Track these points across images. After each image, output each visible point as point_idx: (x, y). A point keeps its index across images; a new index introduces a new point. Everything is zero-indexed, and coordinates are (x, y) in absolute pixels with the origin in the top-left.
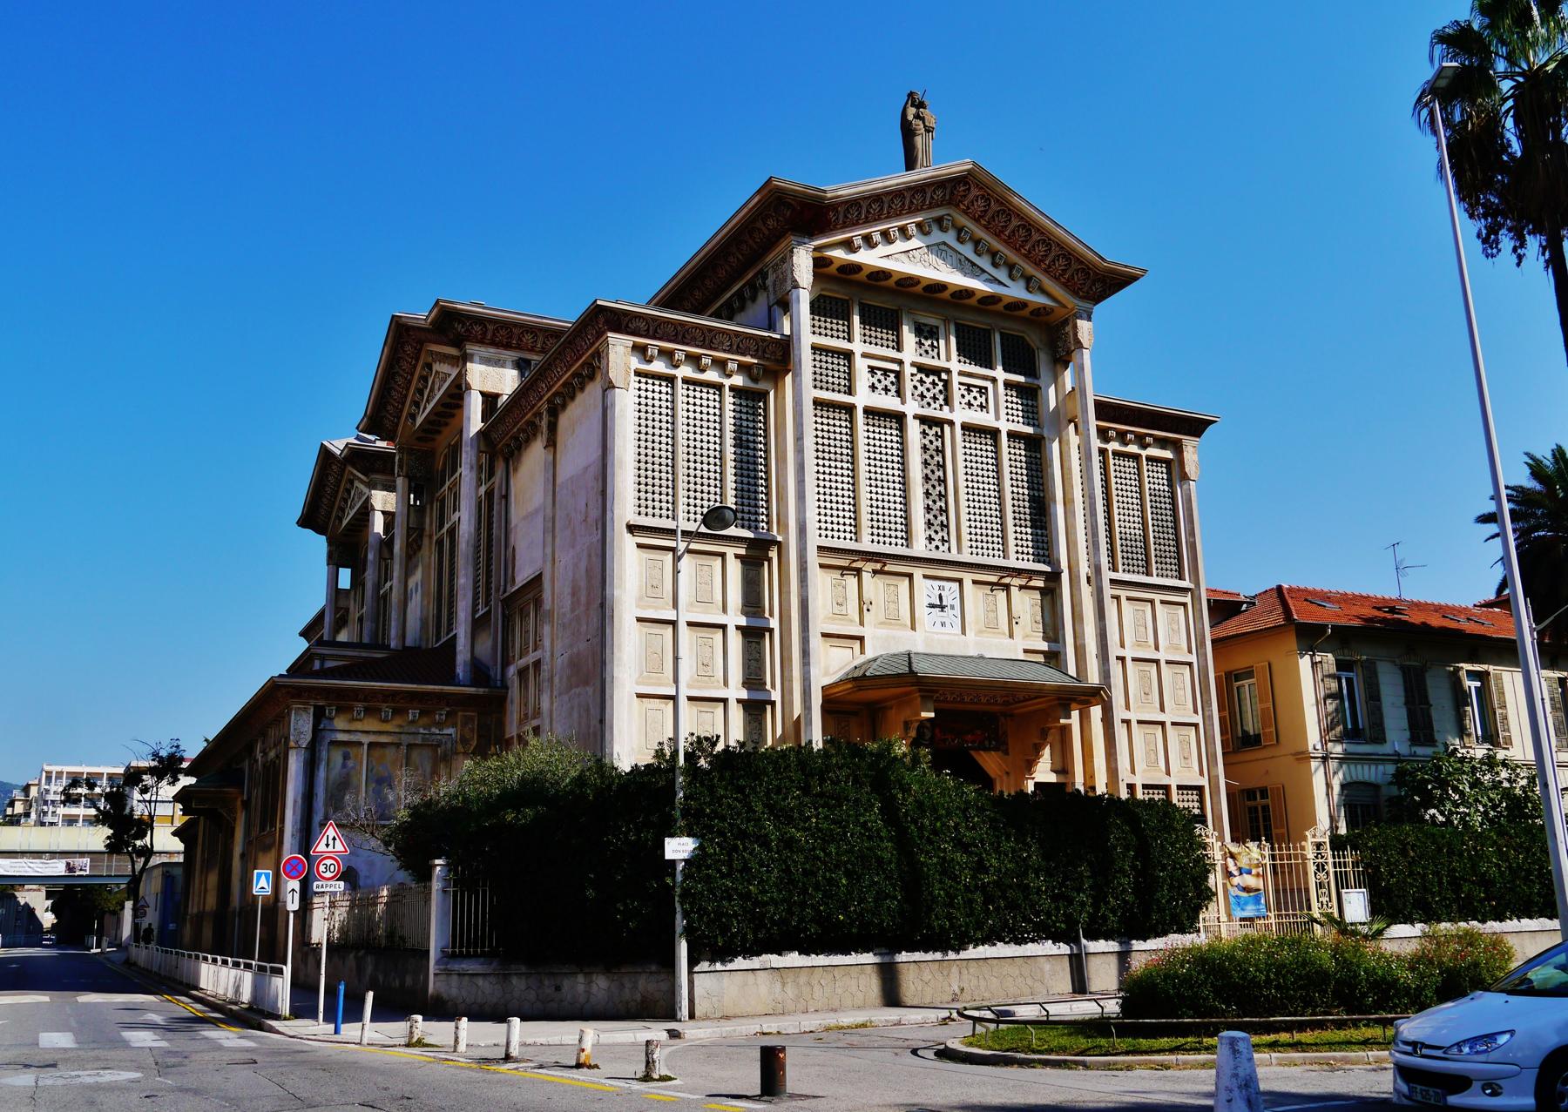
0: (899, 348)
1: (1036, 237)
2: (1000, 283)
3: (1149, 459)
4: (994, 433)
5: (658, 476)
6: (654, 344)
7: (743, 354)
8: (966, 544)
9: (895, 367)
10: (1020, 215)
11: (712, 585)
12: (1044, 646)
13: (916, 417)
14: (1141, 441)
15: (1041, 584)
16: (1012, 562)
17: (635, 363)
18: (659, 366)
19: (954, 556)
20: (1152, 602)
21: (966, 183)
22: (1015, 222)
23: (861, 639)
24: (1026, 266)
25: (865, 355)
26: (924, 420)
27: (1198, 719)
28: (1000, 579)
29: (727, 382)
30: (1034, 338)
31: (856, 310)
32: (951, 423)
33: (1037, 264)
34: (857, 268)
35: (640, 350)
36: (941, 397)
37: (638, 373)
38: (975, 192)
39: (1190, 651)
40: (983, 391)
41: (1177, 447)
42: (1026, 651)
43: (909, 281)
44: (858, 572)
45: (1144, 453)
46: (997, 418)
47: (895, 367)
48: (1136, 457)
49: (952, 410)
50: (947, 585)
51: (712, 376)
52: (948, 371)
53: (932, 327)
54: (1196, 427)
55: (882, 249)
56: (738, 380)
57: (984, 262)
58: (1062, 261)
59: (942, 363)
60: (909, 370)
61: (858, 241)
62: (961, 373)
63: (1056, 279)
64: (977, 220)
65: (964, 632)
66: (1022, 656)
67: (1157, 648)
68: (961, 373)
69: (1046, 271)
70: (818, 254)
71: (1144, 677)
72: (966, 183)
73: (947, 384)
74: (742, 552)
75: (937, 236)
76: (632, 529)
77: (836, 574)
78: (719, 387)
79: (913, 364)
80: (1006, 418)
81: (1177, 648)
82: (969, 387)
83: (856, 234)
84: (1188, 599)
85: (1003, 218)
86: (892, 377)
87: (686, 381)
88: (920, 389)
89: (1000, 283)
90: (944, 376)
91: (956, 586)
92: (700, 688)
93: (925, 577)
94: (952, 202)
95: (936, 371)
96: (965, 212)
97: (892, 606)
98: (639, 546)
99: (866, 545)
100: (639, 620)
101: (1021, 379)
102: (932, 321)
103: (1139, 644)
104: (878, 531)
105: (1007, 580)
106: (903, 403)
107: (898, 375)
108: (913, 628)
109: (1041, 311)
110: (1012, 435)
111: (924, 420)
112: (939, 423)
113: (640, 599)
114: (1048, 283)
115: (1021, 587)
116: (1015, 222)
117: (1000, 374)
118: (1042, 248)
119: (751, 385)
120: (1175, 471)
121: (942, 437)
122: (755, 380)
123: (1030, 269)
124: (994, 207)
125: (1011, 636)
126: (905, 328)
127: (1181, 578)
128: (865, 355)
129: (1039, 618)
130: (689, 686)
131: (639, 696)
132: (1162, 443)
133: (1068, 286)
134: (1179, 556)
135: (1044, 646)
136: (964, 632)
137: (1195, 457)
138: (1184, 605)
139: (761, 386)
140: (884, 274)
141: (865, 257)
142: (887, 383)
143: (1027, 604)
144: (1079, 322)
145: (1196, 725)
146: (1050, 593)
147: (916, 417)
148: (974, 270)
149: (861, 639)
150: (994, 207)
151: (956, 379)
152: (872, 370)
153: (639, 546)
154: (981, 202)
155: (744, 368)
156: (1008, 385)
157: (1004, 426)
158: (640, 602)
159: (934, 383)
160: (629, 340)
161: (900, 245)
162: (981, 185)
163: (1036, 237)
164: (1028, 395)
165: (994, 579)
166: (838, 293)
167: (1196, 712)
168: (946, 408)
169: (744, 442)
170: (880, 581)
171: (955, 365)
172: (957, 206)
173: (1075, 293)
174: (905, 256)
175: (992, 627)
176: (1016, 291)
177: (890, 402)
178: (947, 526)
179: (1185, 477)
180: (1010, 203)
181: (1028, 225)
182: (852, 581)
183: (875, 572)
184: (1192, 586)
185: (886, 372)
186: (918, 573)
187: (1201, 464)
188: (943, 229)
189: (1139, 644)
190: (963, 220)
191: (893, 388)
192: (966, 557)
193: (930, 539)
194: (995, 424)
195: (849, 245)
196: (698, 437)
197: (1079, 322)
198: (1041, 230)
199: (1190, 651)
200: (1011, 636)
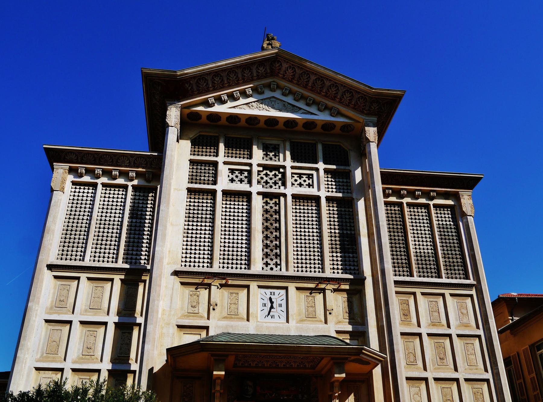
0: (250, 157)
1: (328, 83)
2: (312, 114)
3: (435, 206)
4: (317, 199)
5: (75, 237)
6: (82, 167)
7: (138, 167)
8: (291, 264)
9: (248, 168)
10: (315, 73)
11: (100, 300)
12: (349, 328)
13: (259, 193)
14: (427, 195)
15: (347, 287)
16: (328, 274)
17: (71, 178)
18: (87, 179)
19: (284, 272)
20: (443, 295)
21: (279, 62)
22: (313, 78)
23: (207, 328)
24: (327, 102)
25: (225, 163)
26: (265, 195)
27: (489, 376)
28: (317, 286)
29: (130, 184)
30: (346, 145)
31: (222, 140)
32: (285, 195)
33: (333, 99)
34: (216, 116)
35: (71, 171)
36: (280, 182)
37: (74, 183)
38: (285, 66)
39: (478, 327)
40: (310, 176)
41: (457, 197)
42: (338, 332)
43: (252, 119)
44: (209, 286)
45: (431, 203)
46: (319, 189)
47: (248, 168)
48: (427, 206)
49: (285, 187)
50: (277, 291)
51: (121, 181)
52: (284, 167)
53: (275, 145)
54: (470, 183)
55: (230, 104)
56: (135, 182)
57: (301, 104)
58: (348, 95)
59: (281, 163)
60: (255, 169)
61: (212, 101)
62: (292, 168)
63: (347, 106)
64: (291, 81)
65: (288, 321)
66: (334, 335)
67: (449, 326)
68: (292, 168)
69: (341, 102)
70: (187, 111)
71: (439, 347)
72: (279, 62)
73: (284, 174)
74: (123, 277)
75: (268, 94)
76: (51, 267)
77: (193, 288)
78: (125, 187)
79: (259, 165)
80: (324, 188)
81: (467, 326)
82: (300, 176)
83: (210, 97)
84: (473, 292)
85: (333, 89)
86: (246, 174)
87: (104, 185)
88: (265, 178)
89: (312, 114)
90: (281, 170)
91: (283, 292)
92: (80, 363)
93: (260, 287)
94: (273, 74)
95: (276, 168)
96: (283, 78)
97: (233, 306)
98: (56, 277)
99: (216, 268)
100: (47, 321)
101: (334, 167)
102: (275, 142)
103: (433, 324)
104: (226, 259)
105: (322, 286)
106: (251, 186)
107: (250, 172)
108: (248, 320)
109: (345, 127)
110: (328, 199)
111: (265, 195)
112: (277, 196)
113: (51, 308)
114: (343, 109)
115: (335, 290)
116: (313, 78)
117: (321, 166)
118: (333, 89)
119: (146, 184)
120: (457, 213)
121: (279, 204)
122: (148, 181)
123: (330, 104)
124: (298, 71)
125: (326, 322)
126: (255, 148)
127: (467, 278)
128: (225, 163)
129: (347, 311)
130: (74, 362)
131: (37, 369)
132: (446, 196)
133: (355, 108)
134: (463, 264)
135: (349, 328)
136: (288, 321)
137: (471, 202)
138: (471, 296)
139: (152, 184)
140: (233, 118)
141: (218, 108)
142: (242, 177)
143: (338, 302)
144: (367, 128)
145: (487, 381)
146: (355, 293)
147: (259, 193)
148: (294, 109)
149: (207, 328)
150: (298, 71)
151: (289, 171)
152: (232, 171)
153: (56, 277)
154: (290, 71)
155: (139, 175)
156: (326, 171)
157: (323, 194)
158: (50, 310)
159: (275, 175)
160: (67, 166)
161: (242, 101)
162: (287, 61)
163: (328, 83)
164: (341, 177)
165: (312, 286)
166: (211, 133)
167: (486, 370)
168: (282, 188)
169: (137, 213)
170: (225, 292)
171: (289, 163)
172: (278, 76)
173: (362, 112)
174: (247, 106)
175: (311, 316)
176: (324, 117)
177: (244, 187)
178: (280, 256)
179: (464, 215)
180: (306, 67)
181: (321, 78)
182: (204, 293)
183: (222, 286)
184: (475, 283)
185: (241, 172)
186: (254, 285)
187: (476, 205)
188: (273, 90)
189: (433, 324)
190: (283, 83)
191: (246, 180)
192: (291, 272)
193: (267, 264)
194: (317, 193)
195: (206, 103)
196: (108, 215)
197: (367, 128)
198: (329, 78)
199: (478, 327)
200: (326, 322)
